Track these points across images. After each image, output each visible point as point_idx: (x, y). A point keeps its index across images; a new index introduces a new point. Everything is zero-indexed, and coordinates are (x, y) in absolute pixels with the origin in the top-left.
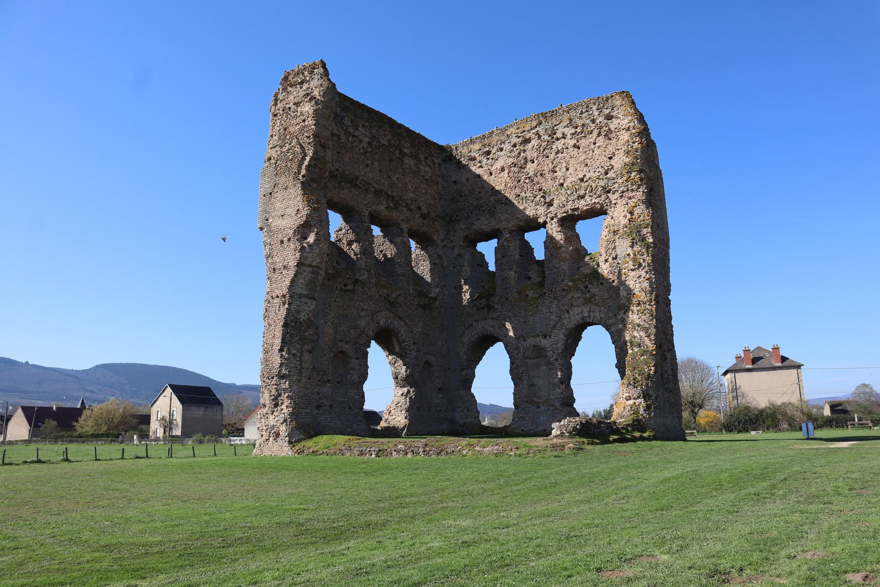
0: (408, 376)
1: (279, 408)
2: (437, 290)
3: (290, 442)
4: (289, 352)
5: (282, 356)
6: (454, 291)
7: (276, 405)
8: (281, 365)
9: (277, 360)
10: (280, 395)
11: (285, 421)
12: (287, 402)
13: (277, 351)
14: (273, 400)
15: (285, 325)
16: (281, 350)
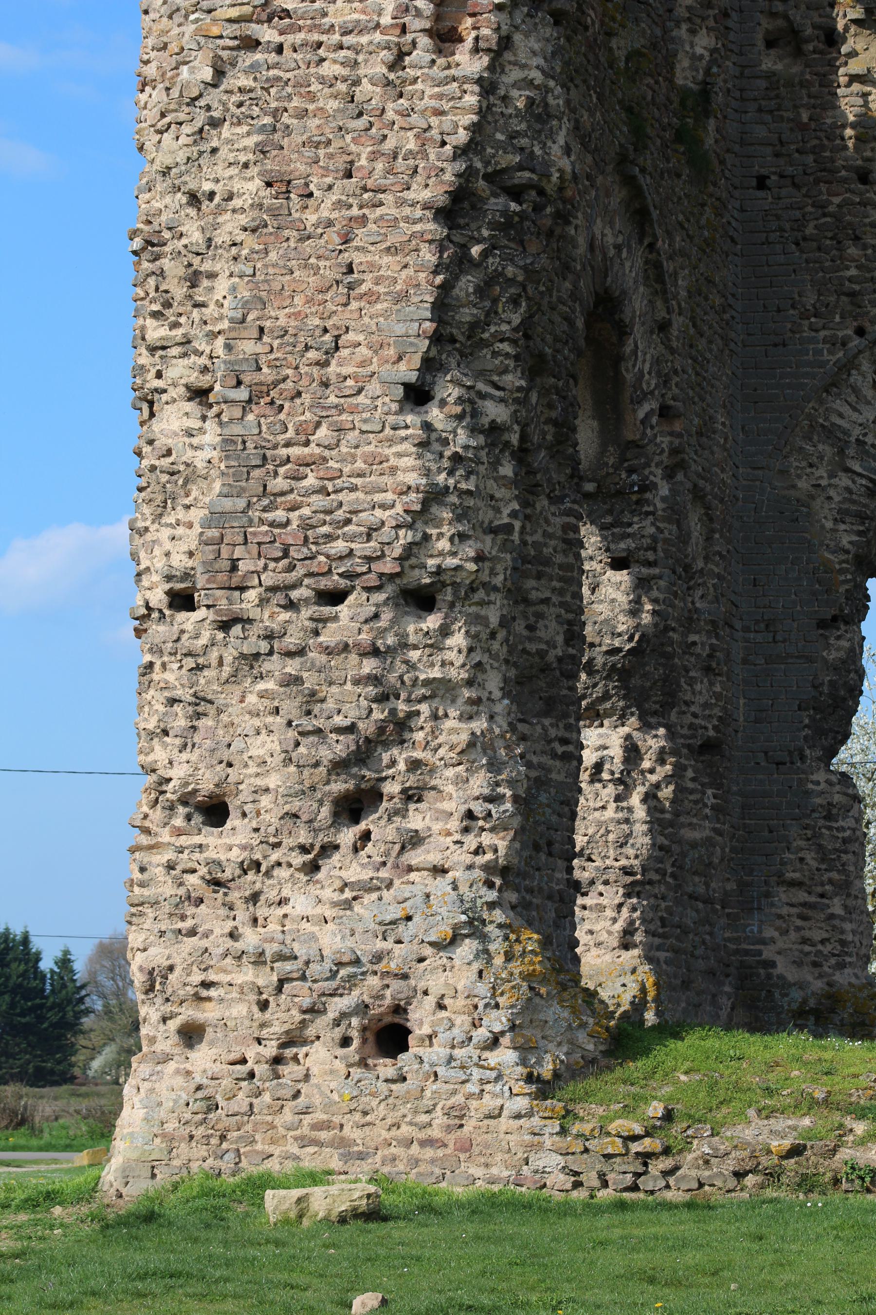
0: (647, 647)
1: (380, 826)
2: (703, 43)
3: (543, 1088)
4: (469, 410)
5: (429, 441)
6: (770, 62)
7: (353, 807)
8: (434, 496)
9: (379, 468)
10: (398, 729)
11: (474, 927)
12: (458, 789)
13: (381, 399)
14: (339, 766)
15: (455, 210)
16: (417, 395)
